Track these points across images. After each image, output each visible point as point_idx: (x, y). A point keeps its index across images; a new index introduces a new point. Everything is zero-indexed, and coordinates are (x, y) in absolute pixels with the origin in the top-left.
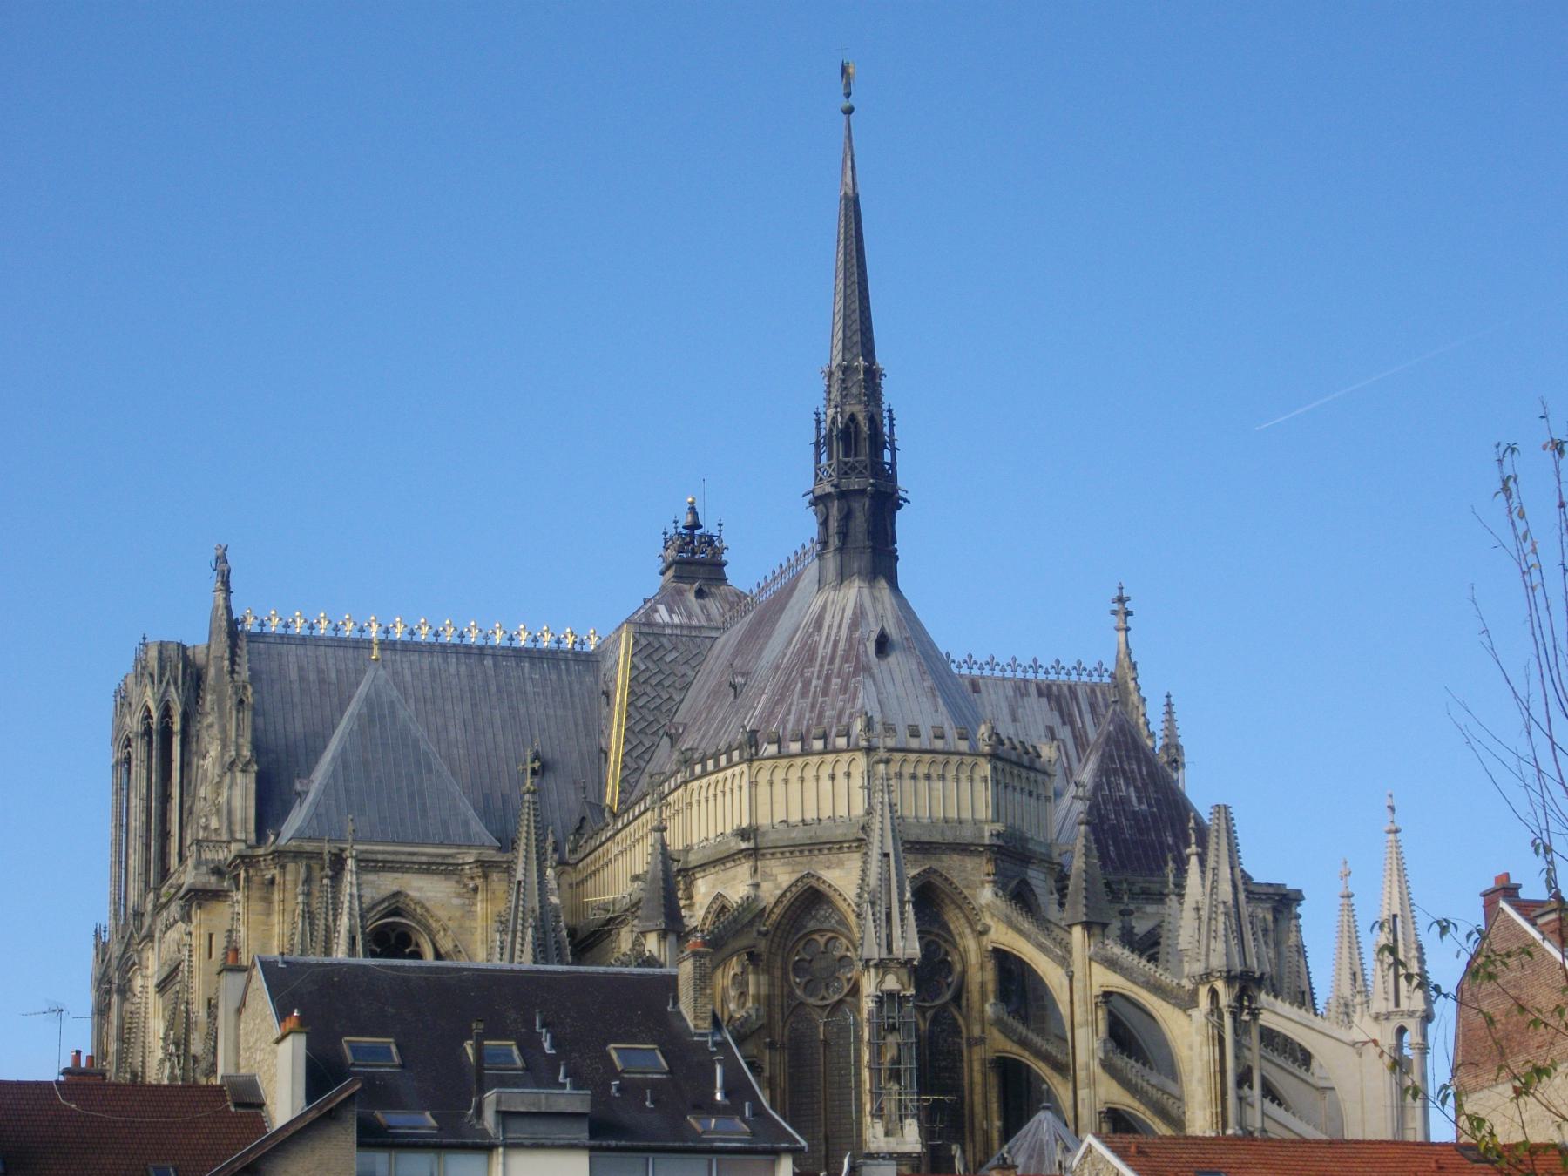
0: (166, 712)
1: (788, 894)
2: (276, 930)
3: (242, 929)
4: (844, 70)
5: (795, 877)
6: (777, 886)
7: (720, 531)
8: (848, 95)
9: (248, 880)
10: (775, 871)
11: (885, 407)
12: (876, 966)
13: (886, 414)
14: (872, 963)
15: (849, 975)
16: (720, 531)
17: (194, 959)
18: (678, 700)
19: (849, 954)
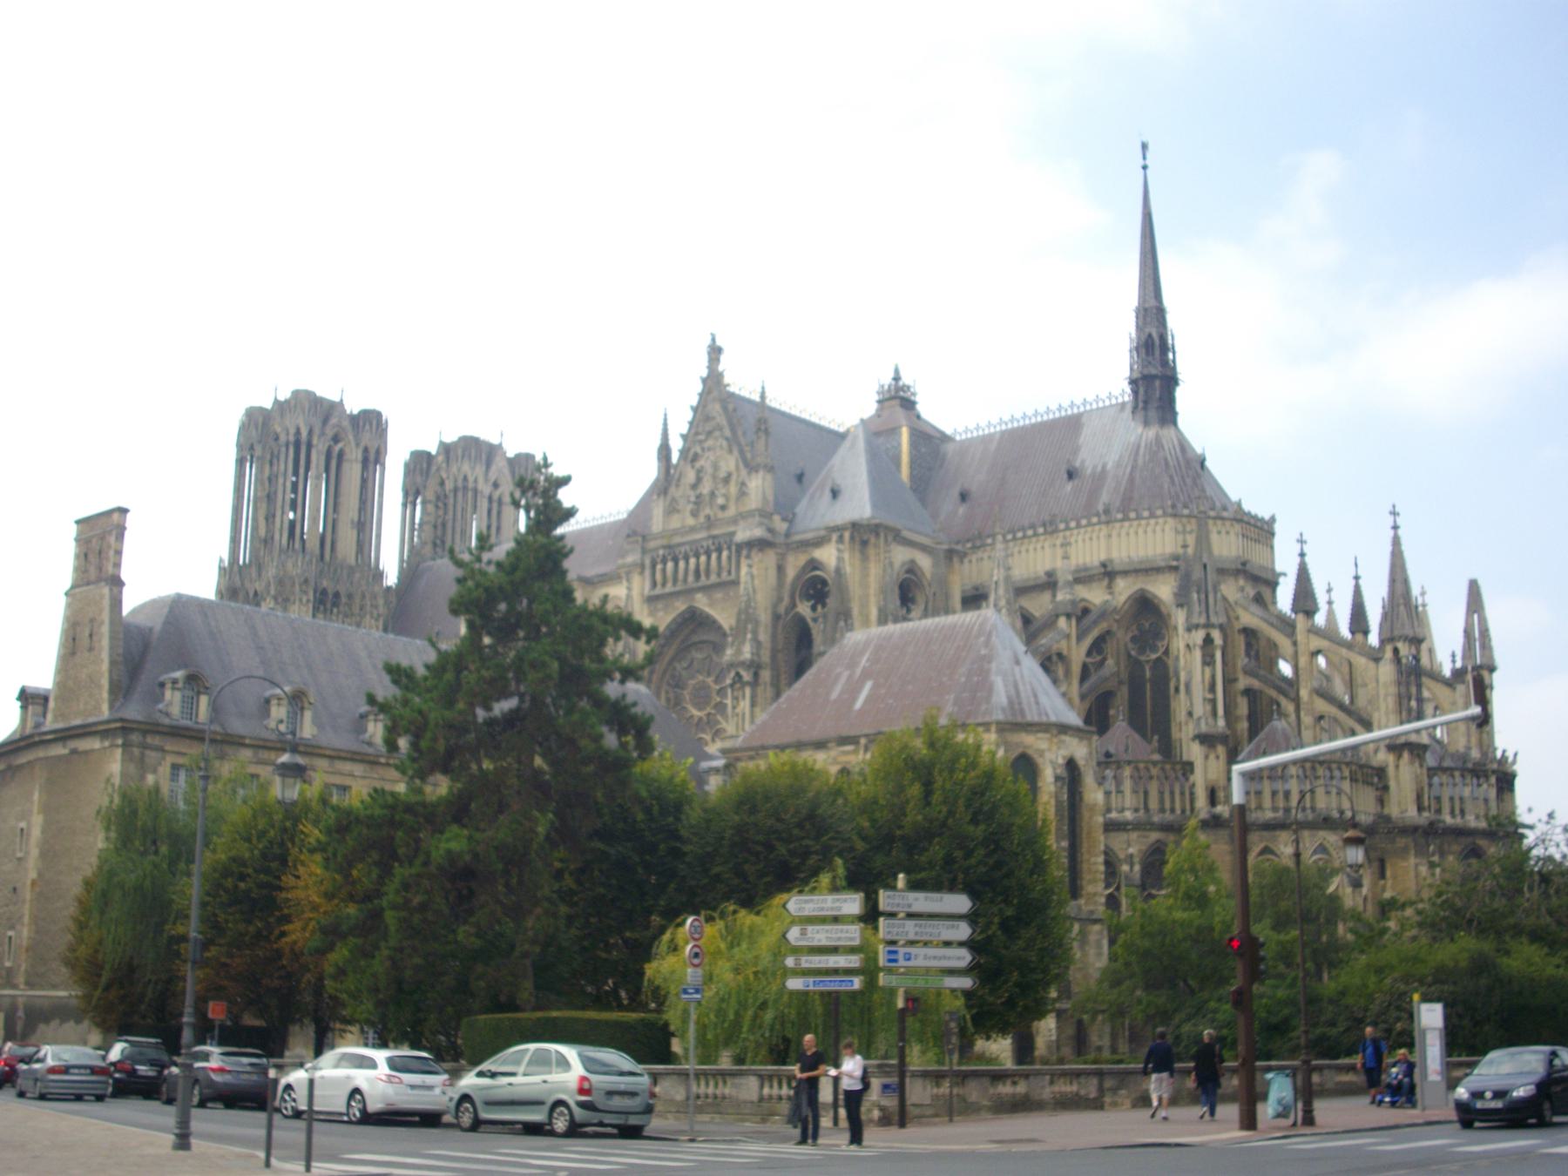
0: (310, 433)
4: (1144, 147)
8: (1144, 158)
9: (852, 538)
17: (756, 582)
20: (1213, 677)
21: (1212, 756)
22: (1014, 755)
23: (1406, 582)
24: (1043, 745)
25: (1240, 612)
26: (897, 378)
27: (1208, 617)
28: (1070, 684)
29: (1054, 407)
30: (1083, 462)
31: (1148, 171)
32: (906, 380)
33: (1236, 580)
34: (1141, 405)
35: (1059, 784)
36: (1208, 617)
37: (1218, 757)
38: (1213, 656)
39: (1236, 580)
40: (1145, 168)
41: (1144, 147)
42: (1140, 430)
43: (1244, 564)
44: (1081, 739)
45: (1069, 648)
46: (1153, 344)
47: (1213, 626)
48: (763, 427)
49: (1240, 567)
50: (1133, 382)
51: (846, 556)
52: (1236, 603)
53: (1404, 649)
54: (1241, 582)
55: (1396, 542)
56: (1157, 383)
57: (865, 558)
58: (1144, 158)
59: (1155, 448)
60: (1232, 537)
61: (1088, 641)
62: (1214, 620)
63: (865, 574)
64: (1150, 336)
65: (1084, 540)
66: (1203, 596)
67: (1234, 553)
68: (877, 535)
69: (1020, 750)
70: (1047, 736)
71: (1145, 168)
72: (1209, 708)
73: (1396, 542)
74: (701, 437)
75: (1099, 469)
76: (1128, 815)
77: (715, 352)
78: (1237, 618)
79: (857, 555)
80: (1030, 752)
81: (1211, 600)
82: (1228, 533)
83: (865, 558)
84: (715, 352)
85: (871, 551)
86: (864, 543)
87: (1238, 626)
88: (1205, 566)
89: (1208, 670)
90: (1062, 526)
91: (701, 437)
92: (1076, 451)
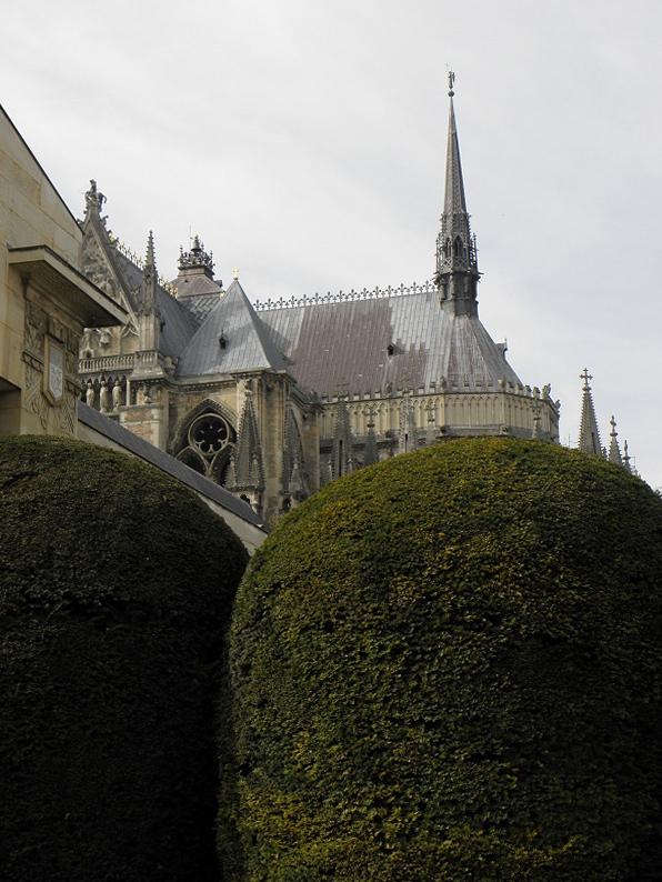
2: (277, 417)
4: (452, 77)
9: (260, 385)
26: (197, 250)
29: (359, 290)
30: (399, 340)
32: (206, 250)
34: (451, 297)
41: (452, 77)
42: (452, 317)
46: (461, 245)
51: (255, 402)
56: (466, 279)
57: (270, 405)
63: (270, 420)
64: (458, 238)
68: (281, 383)
71: (451, 94)
75: (417, 348)
83: (270, 405)
85: (276, 399)
86: (269, 390)
92: (390, 331)
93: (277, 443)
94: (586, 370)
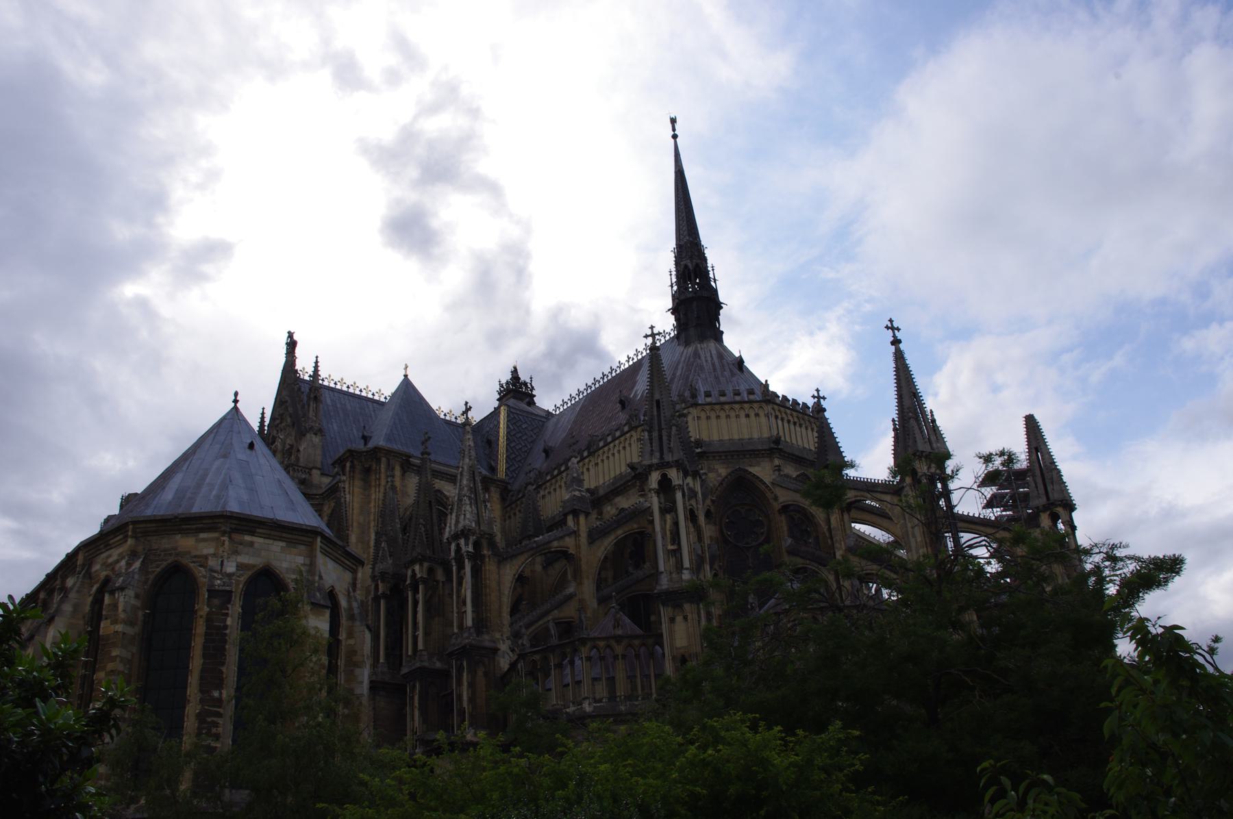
1: (726, 480)
3: (347, 496)
4: (673, 121)
5: (729, 470)
6: (719, 475)
7: (531, 381)
9: (353, 467)
10: (716, 467)
11: (709, 265)
12: (926, 457)
13: (710, 269)
14: (924, 454)
15: (762, 530)
16: (531, 381)
18: (529, 447)
19: (760, 518)
20: (676, 524)
21: (679, 619)
22: (156, 569)
23: (915, 395)
24: (208, 550)
25: (778, 491)
27: (662, 453)
28: (580, 584)
31: (677, 140)
32: (524, 377)
33: (772, 461)
35: (216, 601)
36: (662, 453)
37: (685, 618)
38: (674, 502)
39: (772, 461)
40: (675, 137)
41: (673, 121)
43: (777, 441)
44: (291, 543)
45: (578, 546)
46: (689, 273)
47: (669, 465)
48: (312, 396)
49: (772, 446)
50: (674, 311)
52: (773, 483)
53: (922, 468)
54: (777, 462)
55: (899, 357)
58: (674, 130)
59: (692, 360)
60: (763, 420)
61: (608, 542)
62: (668, 458)
64: (686, 266)
65: (619, 452)
66: (655, 434)
67: (766, 435)
69: (171, 559)
70: (215, 535)
71: (675, 137)
72: (672, 561)
73: (899, 357)
74: (278, 421)
76: (587, 707)
77: (292, 345)
78: (776, 498)
79: (358, 483)
80: (185, 561)
81: (665, 438)
82: (757, 415)
84: (292, 345)
87: (776, 506)
88: (658, 402)
89: (668, 517)
90: (601, 444)
91: (278, 421)
93: (372, 524)
94: (652, 328)
